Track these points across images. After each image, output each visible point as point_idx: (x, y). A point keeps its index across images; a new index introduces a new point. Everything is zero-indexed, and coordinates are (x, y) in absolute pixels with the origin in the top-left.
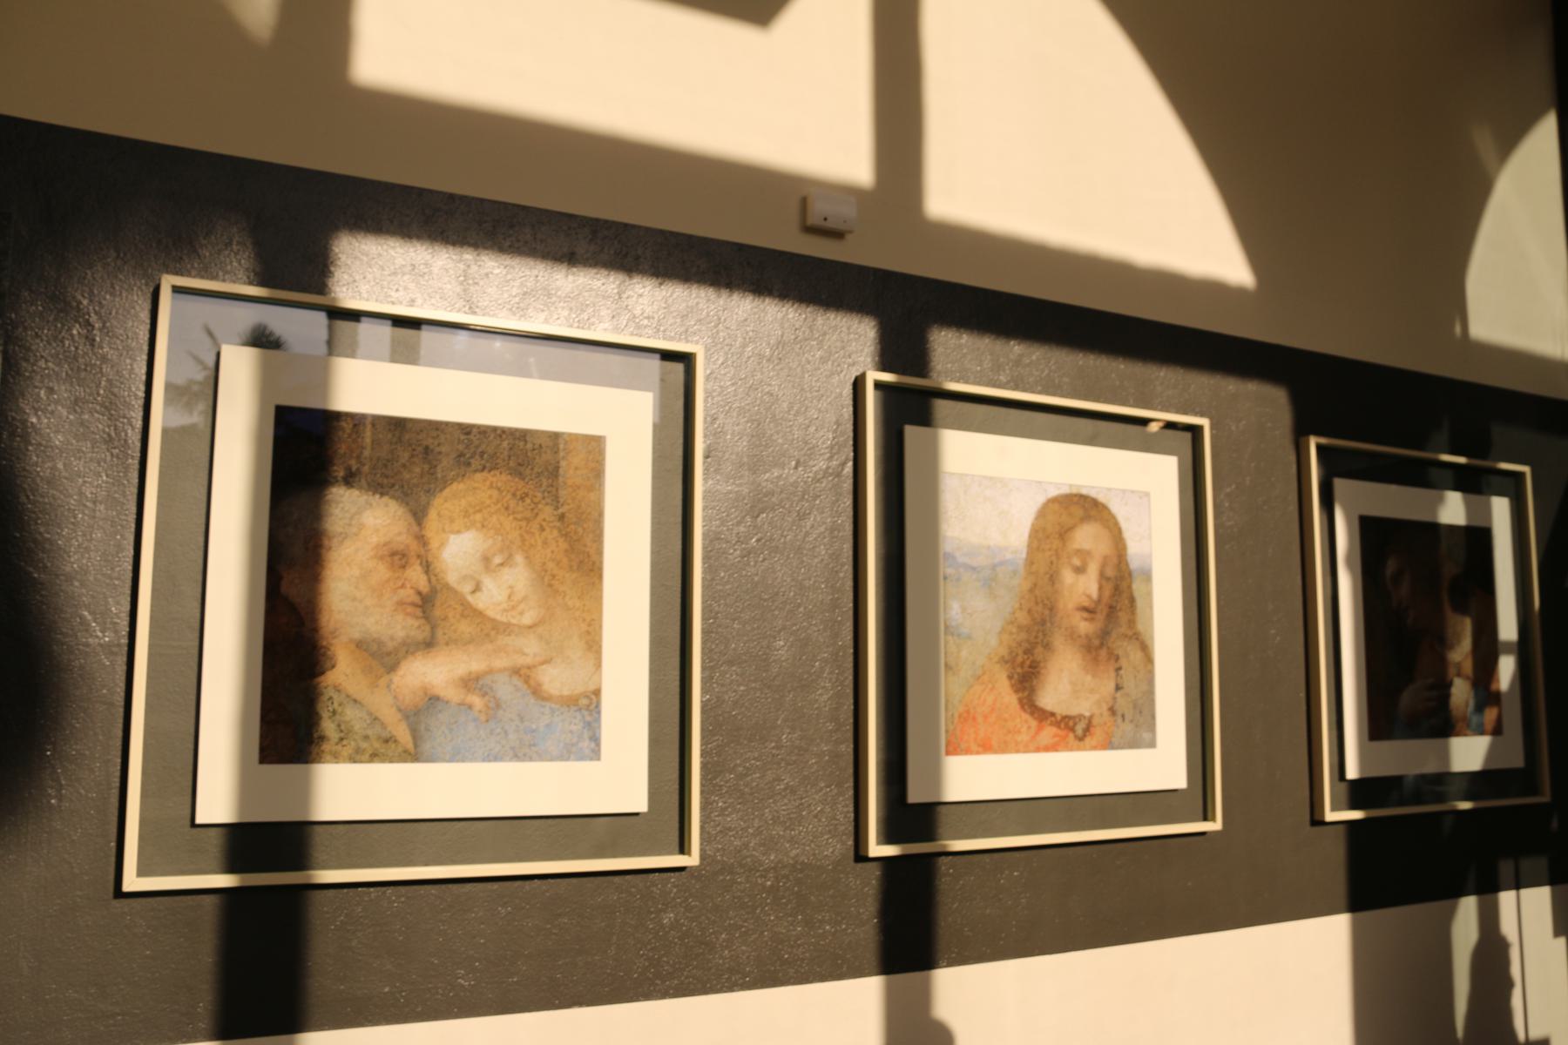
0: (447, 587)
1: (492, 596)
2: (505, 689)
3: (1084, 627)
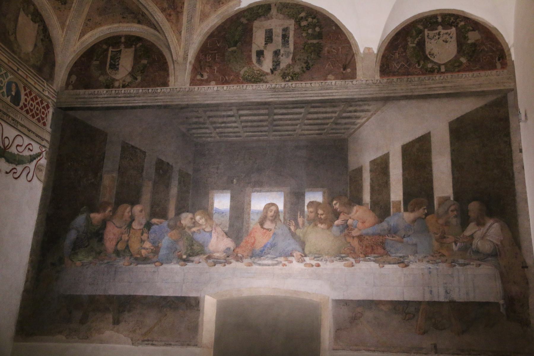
0: (196, 221)
1: (201, 222)
2: (202, 231)
3: (271, 218)
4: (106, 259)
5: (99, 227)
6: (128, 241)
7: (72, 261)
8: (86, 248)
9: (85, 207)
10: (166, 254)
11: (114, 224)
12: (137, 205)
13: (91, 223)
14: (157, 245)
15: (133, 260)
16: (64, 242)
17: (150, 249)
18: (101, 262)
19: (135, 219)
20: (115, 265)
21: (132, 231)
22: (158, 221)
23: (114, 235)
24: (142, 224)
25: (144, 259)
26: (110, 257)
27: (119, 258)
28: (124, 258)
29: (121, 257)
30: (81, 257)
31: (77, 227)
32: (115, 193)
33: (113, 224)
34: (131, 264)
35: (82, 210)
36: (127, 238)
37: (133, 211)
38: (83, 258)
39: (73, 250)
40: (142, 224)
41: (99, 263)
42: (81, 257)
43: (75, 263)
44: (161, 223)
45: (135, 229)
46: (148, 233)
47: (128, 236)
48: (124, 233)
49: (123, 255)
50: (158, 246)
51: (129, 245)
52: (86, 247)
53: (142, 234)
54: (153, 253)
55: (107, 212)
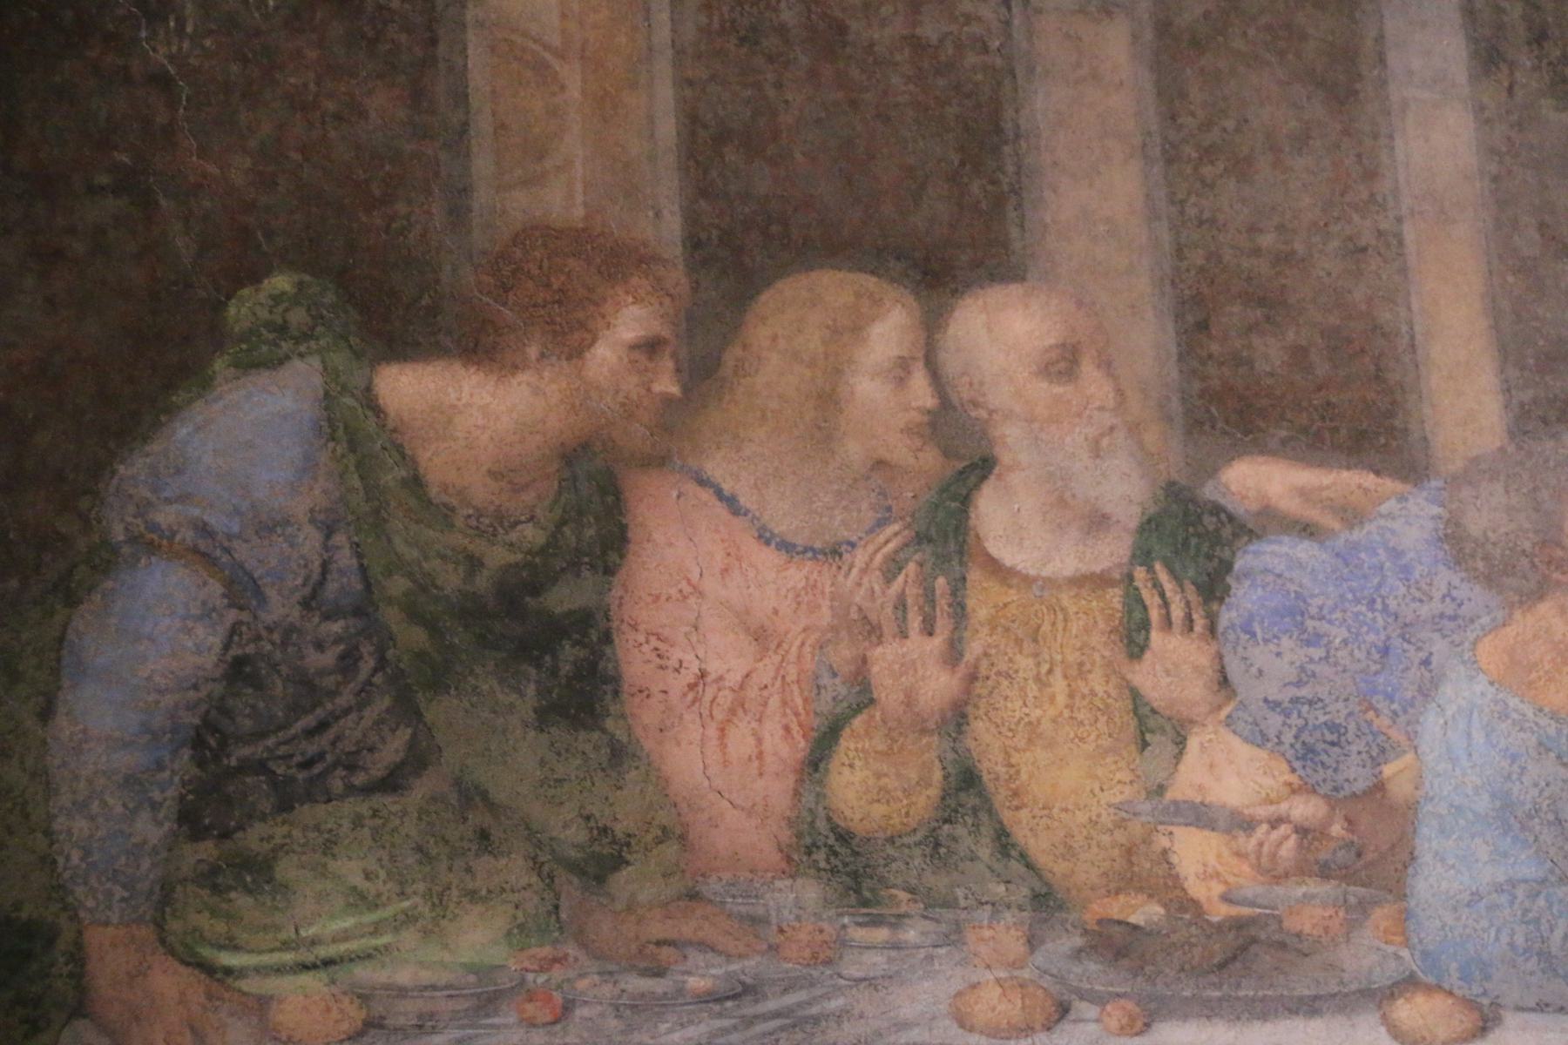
4: (704, 946)
5: (532, 535)
6: (957, 717)
7: (208, 969)
8: (387, 802)
9: (281, 282)
10: (1499, 889)
11: (731, 502)
12: (996, 294)
13: (415, 483)
14: (1357, 776)
15: (1077, 954)
16: (46, 714)
17: (1275, 823)
18: (636, 984)
19: (1005, 458)
20: (840, 1016)
21: (983, 598)
22: (1303, 493)
23: (761, 637)
24: (1097, 522)
25: (1219, 950)
26: (755, 920)
27: (882, 934)
28: (954, 937)
29: (898, 921)
30: (349, 922)
31: (204, 529)
32: (668, 128)
33: (721, 510)
34: (1063, 1010)
35: (243, 310)
36: (938, 686)
37: (951, 363)
38: (376, 930)
39: (190, 822)
40: (1097, 522)
41: (607, 990)
42: (349, 922)
43: (263, 1003)
44: (1352, 515)
45: (1028, 581)
46: (1212, 629)
47: (953, 654)
48: (886, 616)
49: (934, 903)
50: (1379, 787)
51: (991, 765)
52: (391, 783)
53: (1135, 646)
54: (1325, 872)
55: (605, 356)
